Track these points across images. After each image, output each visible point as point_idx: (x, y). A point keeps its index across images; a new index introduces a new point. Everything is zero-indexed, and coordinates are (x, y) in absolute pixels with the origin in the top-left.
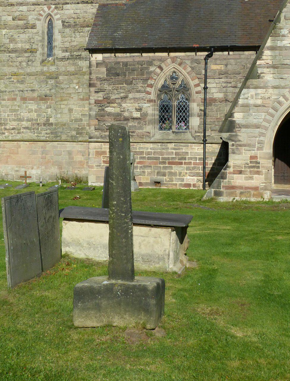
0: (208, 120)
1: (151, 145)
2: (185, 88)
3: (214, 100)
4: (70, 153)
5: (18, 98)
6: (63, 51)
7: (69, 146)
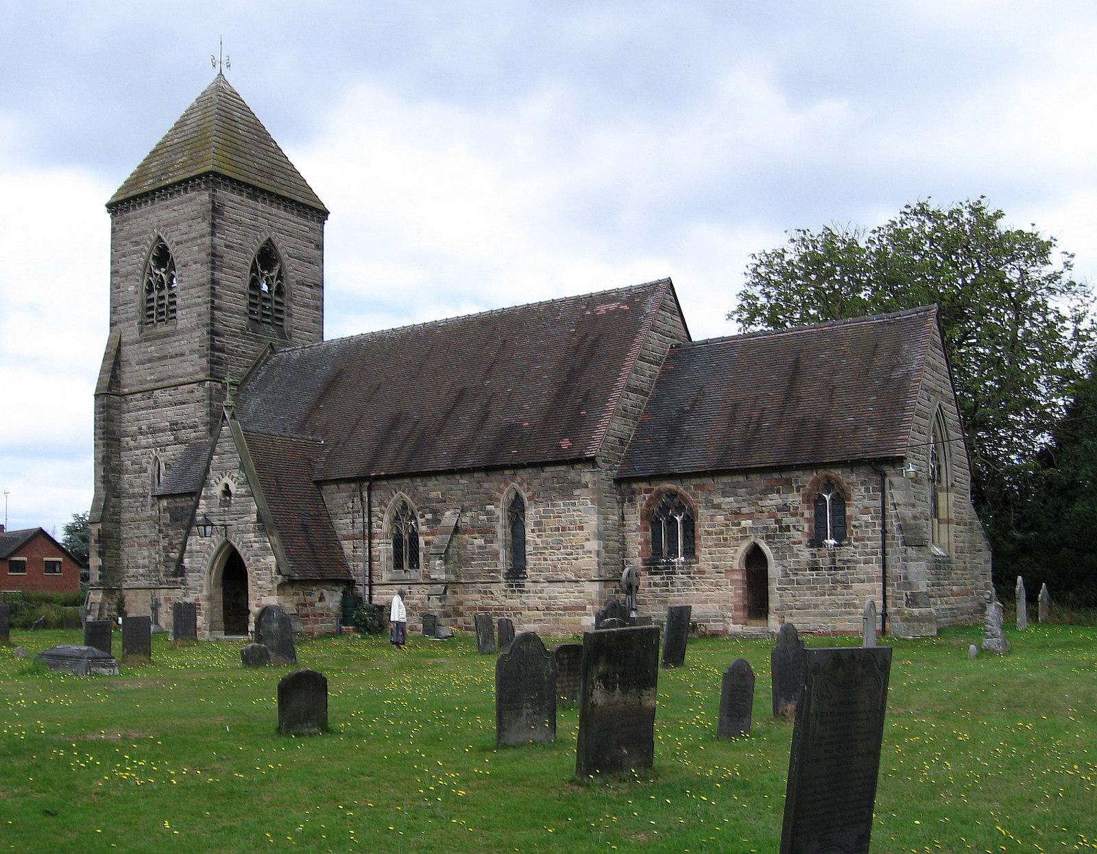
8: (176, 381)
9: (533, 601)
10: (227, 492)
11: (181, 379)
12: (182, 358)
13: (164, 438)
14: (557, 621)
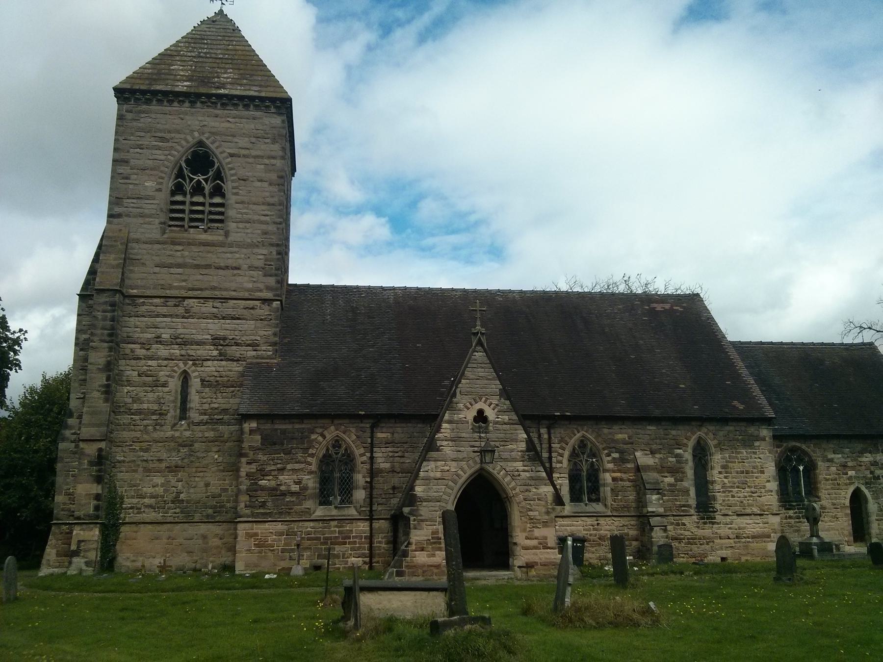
0: (375, 492)
1: (312, 524)
2: (349, 459)
3: (381, 471)
4: (204, 537)
5: (141, 469)
6: (201, 414)
7: (203, 528)
8: (225, 294)
9: (724, 531)
10: (481, 417)
11: (234, 293)
12: (235, 272)
13: (199, 353)
14: (746, 547)
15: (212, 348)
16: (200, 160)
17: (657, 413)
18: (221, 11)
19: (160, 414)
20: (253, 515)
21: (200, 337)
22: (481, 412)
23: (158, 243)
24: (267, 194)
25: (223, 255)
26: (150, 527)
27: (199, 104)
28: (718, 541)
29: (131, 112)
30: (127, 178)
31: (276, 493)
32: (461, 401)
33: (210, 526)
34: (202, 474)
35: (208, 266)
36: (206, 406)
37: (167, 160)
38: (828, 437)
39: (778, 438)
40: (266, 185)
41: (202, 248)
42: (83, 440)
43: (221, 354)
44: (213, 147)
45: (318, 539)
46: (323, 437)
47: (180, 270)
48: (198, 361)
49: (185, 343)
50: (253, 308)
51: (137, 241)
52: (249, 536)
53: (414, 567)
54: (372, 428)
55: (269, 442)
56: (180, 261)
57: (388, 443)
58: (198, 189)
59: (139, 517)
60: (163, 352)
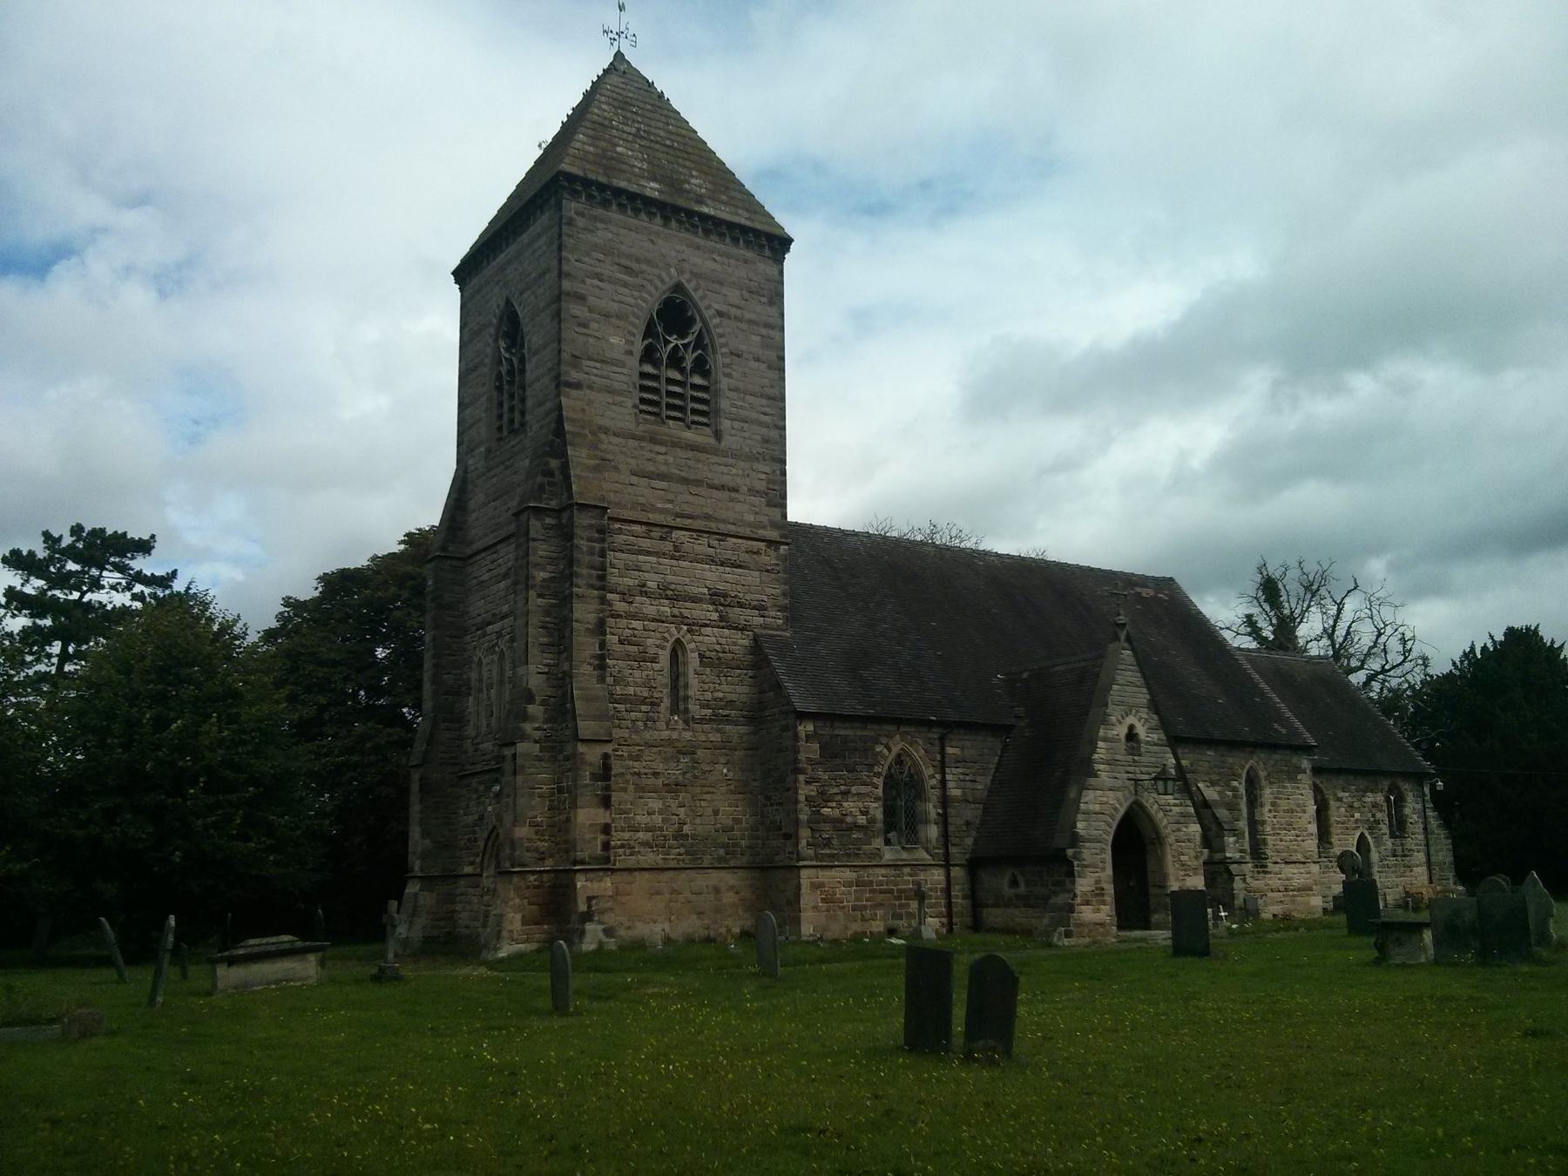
0: (951, 829)
1: (883, 871)
3: (956, 800)
4: (717, 890)
5: (631, 788)
6: (702, 707)
7: (715, 877)
8: (723, 528)
9: (1274, 882)
10: (1131, 736)
11: (732, 528)
12: (734, 495)
13: (696, 613)
14: (1293, 902)
15: (711, 608)
16: (675, 313)
17: (1217, 734)
18: (619, 56)
19: (652, 704)
20: (817, 857)
21: (695, 590)
22: (1131, 727)
23: (634, 437)
24: (766, 381)
25: (716, 468)
26: (646, 875)
27: (674, 224)
28: (1270, 894)
29: (582, 214)
30: (585, 326)
31: (840, 825)
32: (1114, 712)
33: (723, 874)
34: (708, 797)
35: (698, 483)
36: (708, 696)
37: (637, 306)
38: (1339, 772)
39: (1317, 771)
40: (763, 366)
41: (690, 454)
42: (583, 741)
43: (722, 618)
44: (696, 296)
45: (891, 892)
46: (889, 748)
47: (664, 484)
48: (694, 626)
49: (675, 598)
50: (758, 553)
51: (606, 431)
52: (817, 886)
53: (1080, 925)
54: (942, 739)
55: (832, 753)
56: (663, 469)
57: (960, 761)
58: (675, 360)
59: (632, 861)
60: (650, 609)
